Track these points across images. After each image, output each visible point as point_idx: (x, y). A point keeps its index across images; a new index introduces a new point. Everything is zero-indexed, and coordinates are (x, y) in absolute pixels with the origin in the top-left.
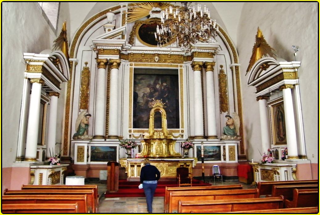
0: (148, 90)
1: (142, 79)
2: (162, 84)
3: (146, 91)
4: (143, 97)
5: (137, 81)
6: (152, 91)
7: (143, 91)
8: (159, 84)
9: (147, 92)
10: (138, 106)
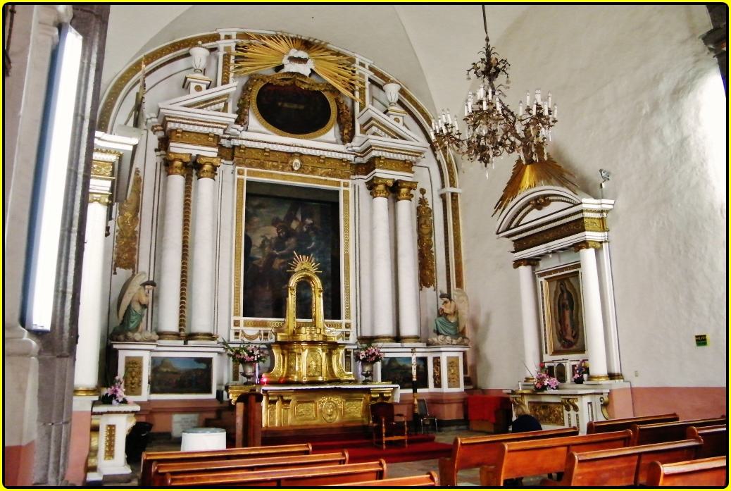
0: (273, 232)
1: (260, 206)
3: (268, 234)
4: (262, 246)
7: (263, 234)
8: (296, 219)
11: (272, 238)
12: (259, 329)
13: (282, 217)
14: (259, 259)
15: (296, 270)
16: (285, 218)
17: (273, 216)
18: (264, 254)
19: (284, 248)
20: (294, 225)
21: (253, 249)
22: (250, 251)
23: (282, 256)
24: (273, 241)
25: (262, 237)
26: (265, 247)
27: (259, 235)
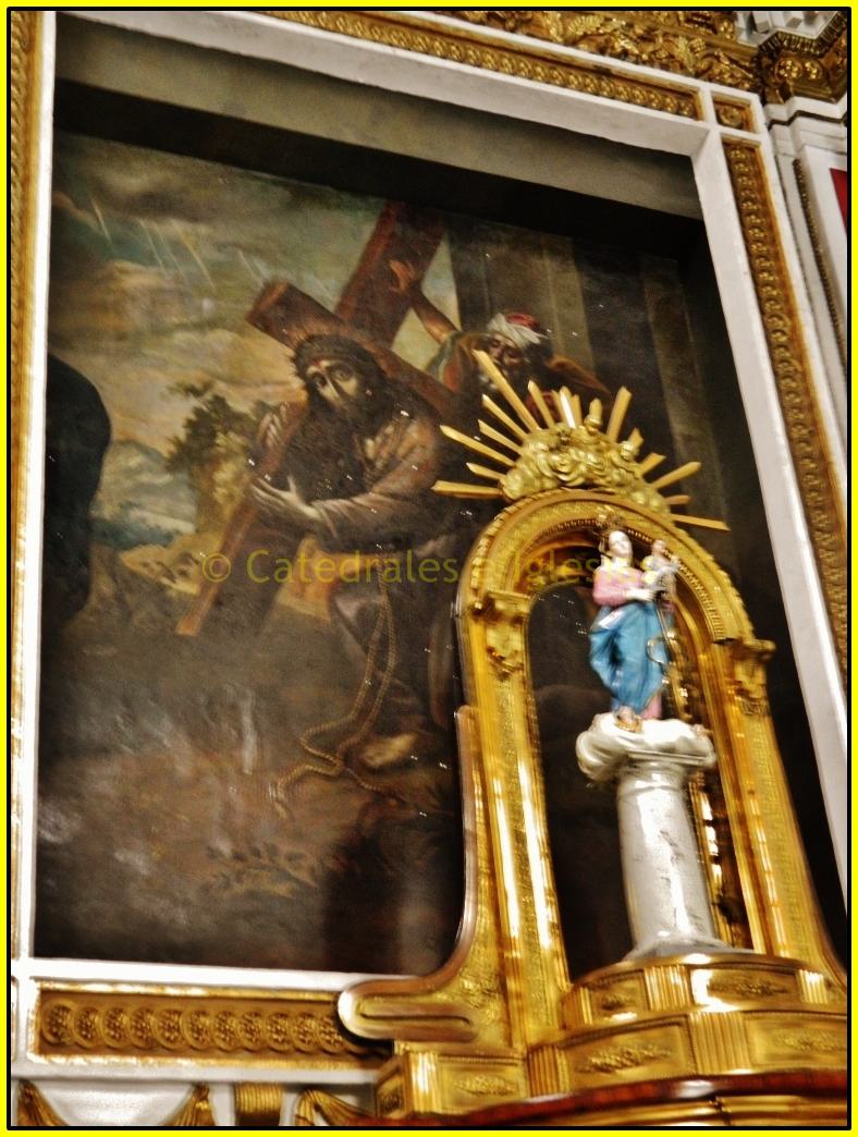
0: (271, 376)
1: (157, 204)
2: (475, 311)
3: (234, 382)
4: (194, 453)
5: (96, 220)
6: (329, 392)
7: (194, 377)
8: (430, 312)
9: (255, 394)
10: (103, 586)
11: (262, 408)
12: (190, 1068)
13: (326, 286)
14: (167, 538)
15: (512, 485)
16: (347, 292)
17: (261, 272)
18: (206, 505)
19: (356, 477)
20: (415, 344)
21: (116, 470)
22: (91, 484)
23: (346, 538)
24: (273, 429)
25: (192, 391)
26: (216, 462)
27: (162, 380)
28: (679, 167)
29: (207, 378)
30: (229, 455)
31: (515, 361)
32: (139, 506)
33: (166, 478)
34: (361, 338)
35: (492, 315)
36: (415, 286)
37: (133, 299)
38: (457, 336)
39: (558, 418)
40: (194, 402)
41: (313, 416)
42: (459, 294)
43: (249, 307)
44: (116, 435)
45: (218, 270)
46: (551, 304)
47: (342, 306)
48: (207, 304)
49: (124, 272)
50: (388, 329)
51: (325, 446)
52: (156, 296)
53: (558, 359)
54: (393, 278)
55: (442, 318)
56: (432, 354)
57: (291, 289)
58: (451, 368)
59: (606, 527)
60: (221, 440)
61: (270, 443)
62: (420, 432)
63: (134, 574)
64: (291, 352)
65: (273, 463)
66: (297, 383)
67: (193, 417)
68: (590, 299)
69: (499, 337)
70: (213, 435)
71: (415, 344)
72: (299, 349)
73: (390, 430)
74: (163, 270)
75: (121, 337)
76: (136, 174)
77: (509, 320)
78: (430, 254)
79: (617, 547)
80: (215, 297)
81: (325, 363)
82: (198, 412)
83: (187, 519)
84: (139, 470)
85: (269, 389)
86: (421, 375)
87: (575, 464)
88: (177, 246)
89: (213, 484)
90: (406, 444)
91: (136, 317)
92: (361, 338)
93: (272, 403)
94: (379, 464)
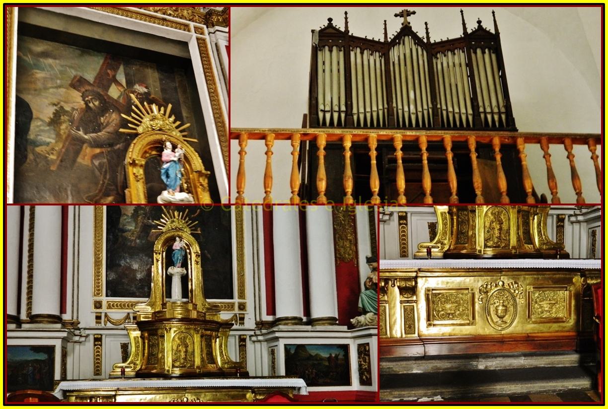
0: (76, 100)
1: (45, 55)
2: (130, 83)
3: (65, 102)
4: (55, 121)
5: (29, 59)
6: (91, 105)
7: (55, 101)
8: (118, 84)
9: (71, 105)
10: (31, 157)
11: (73, 109)
13: (90, 76)
14: (48, 144)
15: (140, 130)
16: (96, 78)
17: (73, 73)
18: (58, 135)
19: (98, 128)
20: (114, 92)
21: (34, 126)
22: (28, 129)
23: (96, 144)
24: (76, 115)
25: (54, 105)
26: (61, 124)
27: (47, 102)
28: (185, 45)
29: (58, 101)
30: (65, 121)
31: (141, 96)
32: (40, 135)
33: (48, 128)
34: (100, 90)
35: (135, 84)
36: (114, 77)
37: (39, 80)
38: (125, 91)
39: (152, 112)
40: (55, 108)
41: (87, 111)
42: (126, 79)
43: (70, 82)
44: (34, 116)
45: (61, 72)
46: (150, 81)
47: (94, 82)
48: (58, 81)
49: (36, 73)
50: (107, 88)
51: (90, 119)
52: (45, 79)
53: (152, 96)
54: (108, 74)
55: (122, 86)
56: (119, 95)
57: (81, 77)
58: (124, 98)
59: (165, 141)
60: (62, 118)
61: (75, 118)
62: (115, 116)
63: (39, 154)
64: (81, 94)
65: (76, 124)
66: (83, 103)
67: (55, 112)
68: (161, 80)
69: (137, 90)
70: (60, 116)
71: (114, 92)
72: (83, 93)
73: (107, 115)
74: (46, 72)
75: (36, 90)
76: (40, 47)
77: (139, 86)
78: (118, 68)
79: (168, 146)
80: (60, 79)
81: (90, 97)
82: (56, 110)
83: (53, 139)
84: (40, 126)
85: (75, 104)
86: (116, 100)
87: (157, 124)
88: (51, 66)
89: (60, 129)
90: (112, 119)
91: (39, 85)
92: (100, 90)
93: (76, 108)
94: (105, 124)
